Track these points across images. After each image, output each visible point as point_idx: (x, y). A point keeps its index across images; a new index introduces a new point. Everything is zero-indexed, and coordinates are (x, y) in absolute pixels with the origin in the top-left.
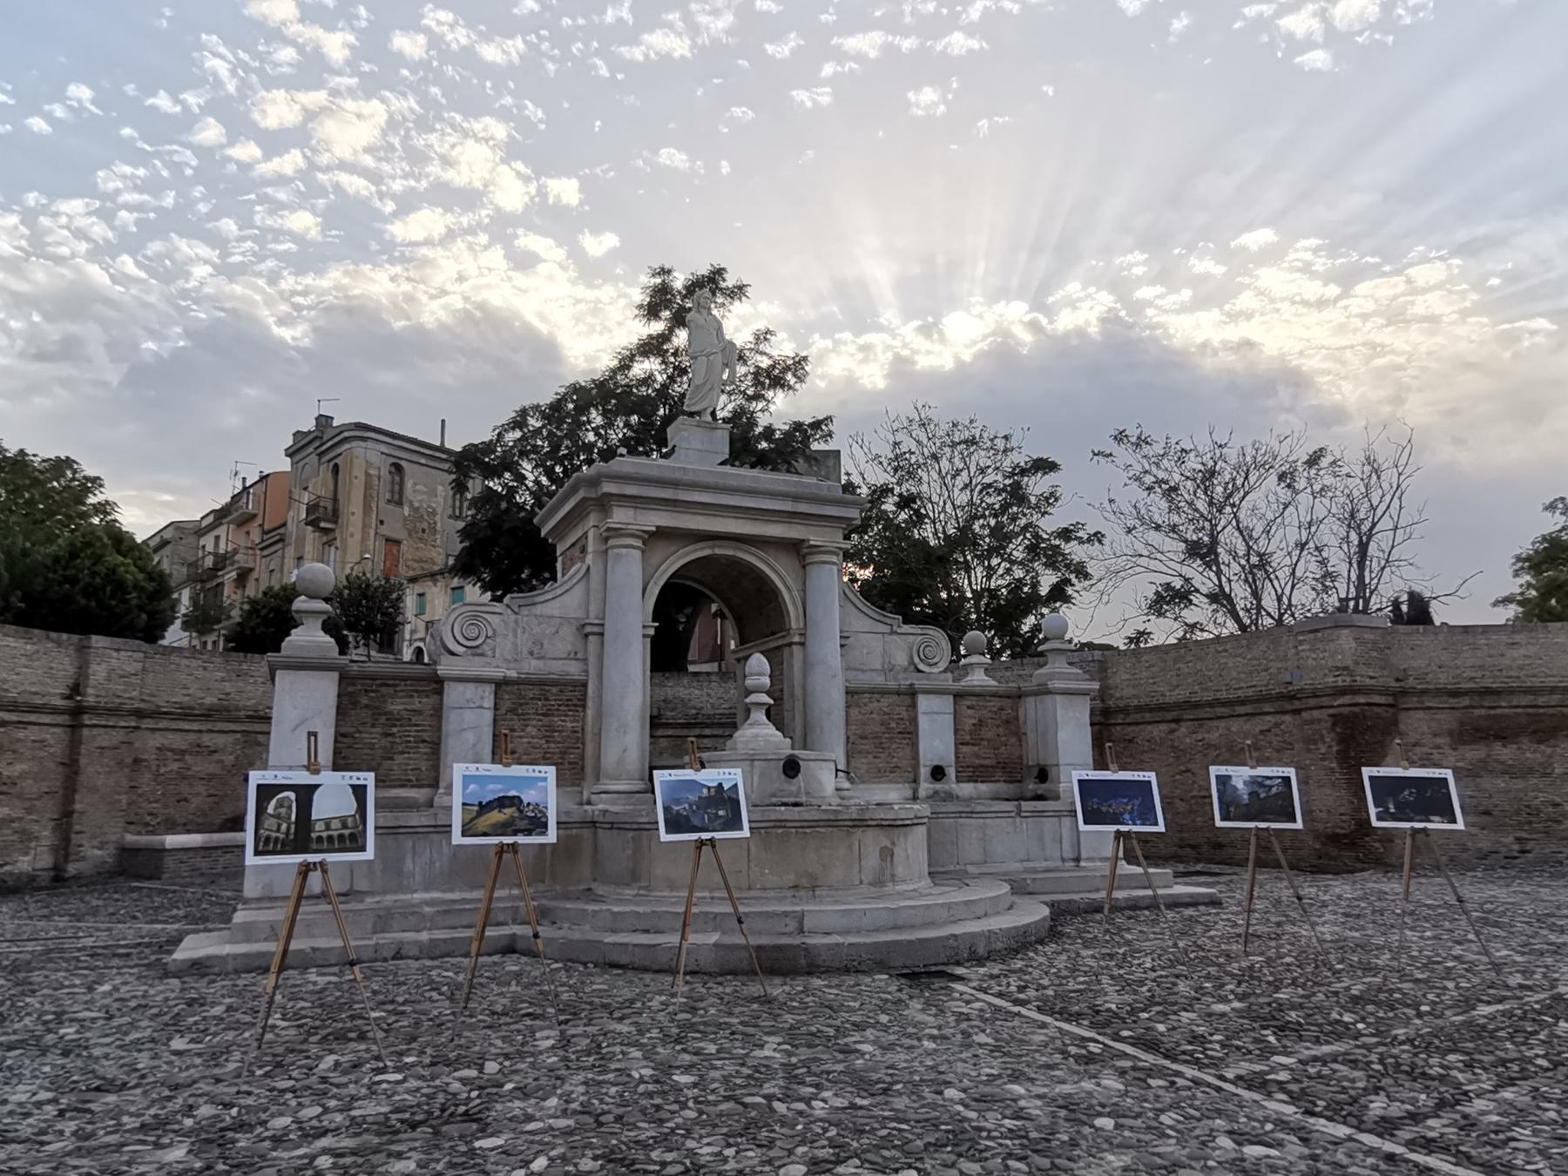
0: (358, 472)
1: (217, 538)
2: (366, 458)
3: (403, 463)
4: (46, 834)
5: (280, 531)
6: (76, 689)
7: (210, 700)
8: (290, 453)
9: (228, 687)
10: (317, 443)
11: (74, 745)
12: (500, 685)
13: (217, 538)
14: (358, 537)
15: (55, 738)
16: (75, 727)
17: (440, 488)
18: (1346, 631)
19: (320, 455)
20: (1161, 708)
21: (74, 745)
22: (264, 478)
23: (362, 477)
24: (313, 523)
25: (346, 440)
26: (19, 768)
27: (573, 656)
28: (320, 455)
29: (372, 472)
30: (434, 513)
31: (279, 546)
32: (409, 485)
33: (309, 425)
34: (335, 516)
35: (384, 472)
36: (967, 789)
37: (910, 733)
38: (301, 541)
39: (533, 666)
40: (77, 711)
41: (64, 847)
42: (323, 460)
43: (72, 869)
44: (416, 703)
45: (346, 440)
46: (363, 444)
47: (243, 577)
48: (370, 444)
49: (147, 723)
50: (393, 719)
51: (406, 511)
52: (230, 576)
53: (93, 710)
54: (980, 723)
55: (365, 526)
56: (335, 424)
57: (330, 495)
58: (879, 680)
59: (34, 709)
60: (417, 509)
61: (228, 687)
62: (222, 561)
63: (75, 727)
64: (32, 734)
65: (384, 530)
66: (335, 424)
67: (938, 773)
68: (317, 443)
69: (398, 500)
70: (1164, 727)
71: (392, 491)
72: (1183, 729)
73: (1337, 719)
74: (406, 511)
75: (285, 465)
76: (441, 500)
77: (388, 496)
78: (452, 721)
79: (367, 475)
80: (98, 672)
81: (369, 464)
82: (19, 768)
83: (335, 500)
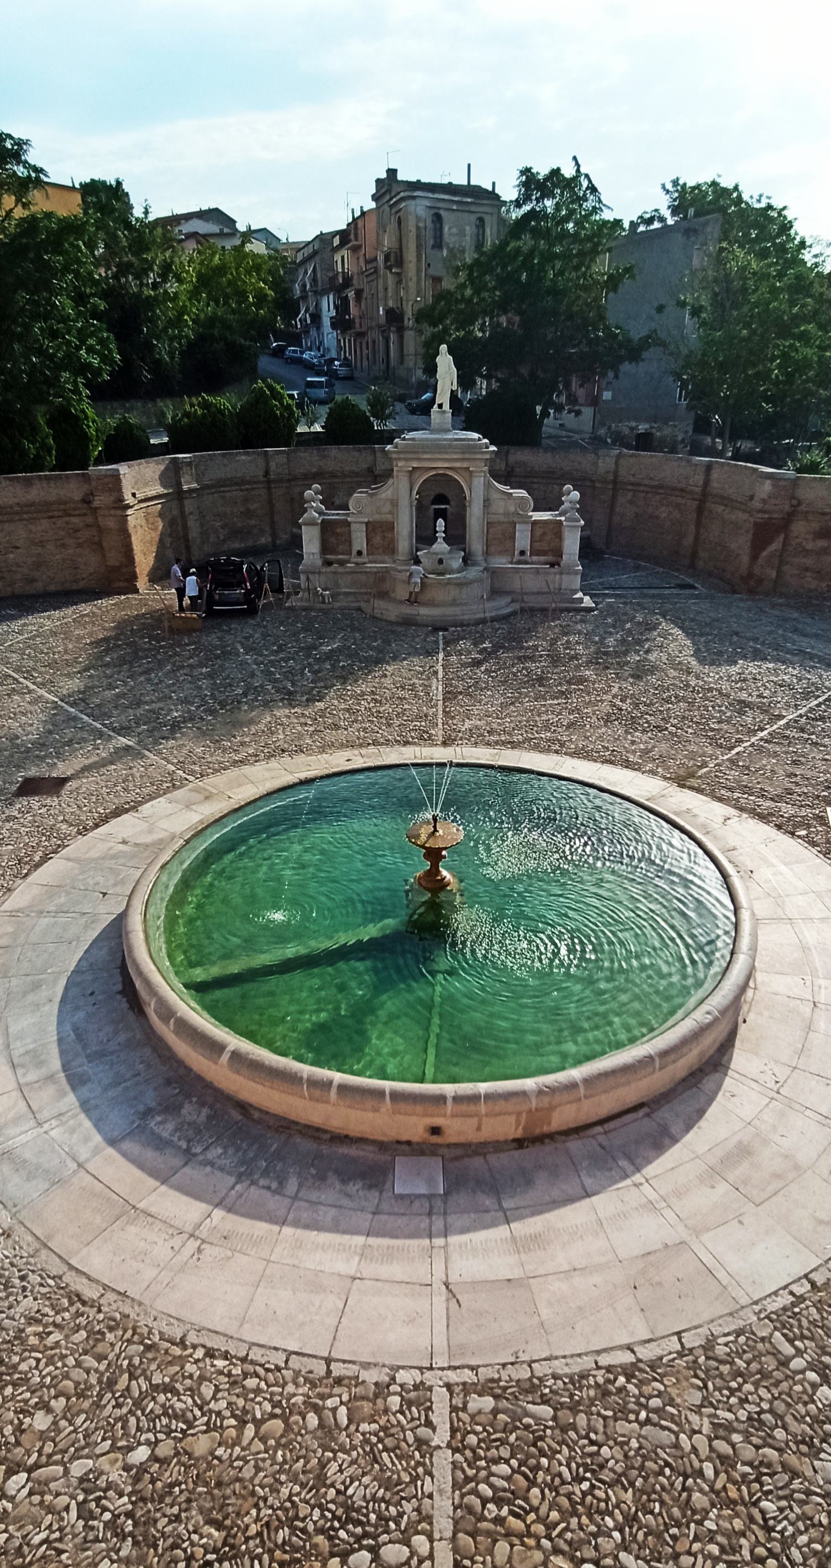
0: (411, 225)
1: (343, 257)
2: (419, 208)
3: (442, 212)
4: (267, 529)
5: (374, 265)
6: (267, 473)
7: (314, 470)
8: (375, 198)
9: (321, 463)
10: (387, 197)
11: (270, 494)
12: (367, 524)
13: (343, 257)
14: (414, 279)
15: (263, 492)
16: (269, 488)
17: (468, 228)
18: (768, 482)
19: (391, 207)
20: (722, 497)
21: (270, 494)
22: (363, 213)
23: (414, 230)
24: (389, 268)
25: (403, 199)
26: (255, 506)
27: (391, 513)
28: (391, 207)
29: (421, 225)
30: (463, 252)
31: (374, 276)
32: (446, 229)
33: (383, 175)
34: (400, 262)
35: (429, 224)
36: (535, 558)
37: (513, 538)
38: (385, 275)
39: (377, 517)
40: (269, 482)
41: (274, 535)
42: (394, 211)
43: (278, 542)
44: (345, 529)
45: (403, 199)
46: (413, 202)
47: (359, 293)
48: (418, 201)
49: (293, 483)
50: (338, 534)
51: (445, 253)
52: (351, 295)
53: (274, 481)
54: (544, 534)
55: (419, 270)
56: (400, 177)
57: (396, 245)
58: (502, 518)
59: (255, 483)
60: (451, 250)
61: (321, 463)
62: (348, 282)
63: (269, 488)
64: (257, 492)
65: (432, 271)
66: (400, 177)
67: (522, 553)
68: (387, 197)
69: (438, 245)
70: (722, 508)
71: (435, 238)
72: (728, 510)
73: (756, 524)
74: (445, 253)
75: (373, 205)
76: (468, 238)
77: (432, 242)
78: (354, 536)
79: (418, 228)
80: (273, 465)
81: (418, 219)
82: (255, 506)
83: (401, 249)
